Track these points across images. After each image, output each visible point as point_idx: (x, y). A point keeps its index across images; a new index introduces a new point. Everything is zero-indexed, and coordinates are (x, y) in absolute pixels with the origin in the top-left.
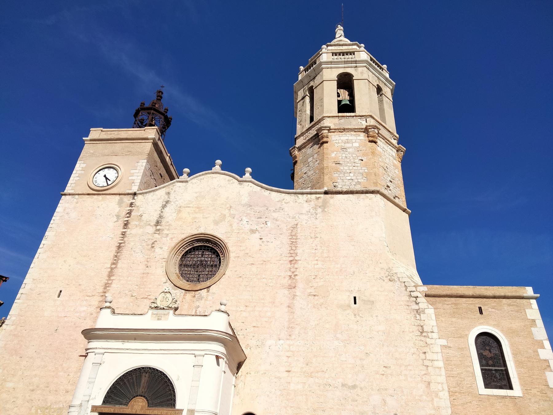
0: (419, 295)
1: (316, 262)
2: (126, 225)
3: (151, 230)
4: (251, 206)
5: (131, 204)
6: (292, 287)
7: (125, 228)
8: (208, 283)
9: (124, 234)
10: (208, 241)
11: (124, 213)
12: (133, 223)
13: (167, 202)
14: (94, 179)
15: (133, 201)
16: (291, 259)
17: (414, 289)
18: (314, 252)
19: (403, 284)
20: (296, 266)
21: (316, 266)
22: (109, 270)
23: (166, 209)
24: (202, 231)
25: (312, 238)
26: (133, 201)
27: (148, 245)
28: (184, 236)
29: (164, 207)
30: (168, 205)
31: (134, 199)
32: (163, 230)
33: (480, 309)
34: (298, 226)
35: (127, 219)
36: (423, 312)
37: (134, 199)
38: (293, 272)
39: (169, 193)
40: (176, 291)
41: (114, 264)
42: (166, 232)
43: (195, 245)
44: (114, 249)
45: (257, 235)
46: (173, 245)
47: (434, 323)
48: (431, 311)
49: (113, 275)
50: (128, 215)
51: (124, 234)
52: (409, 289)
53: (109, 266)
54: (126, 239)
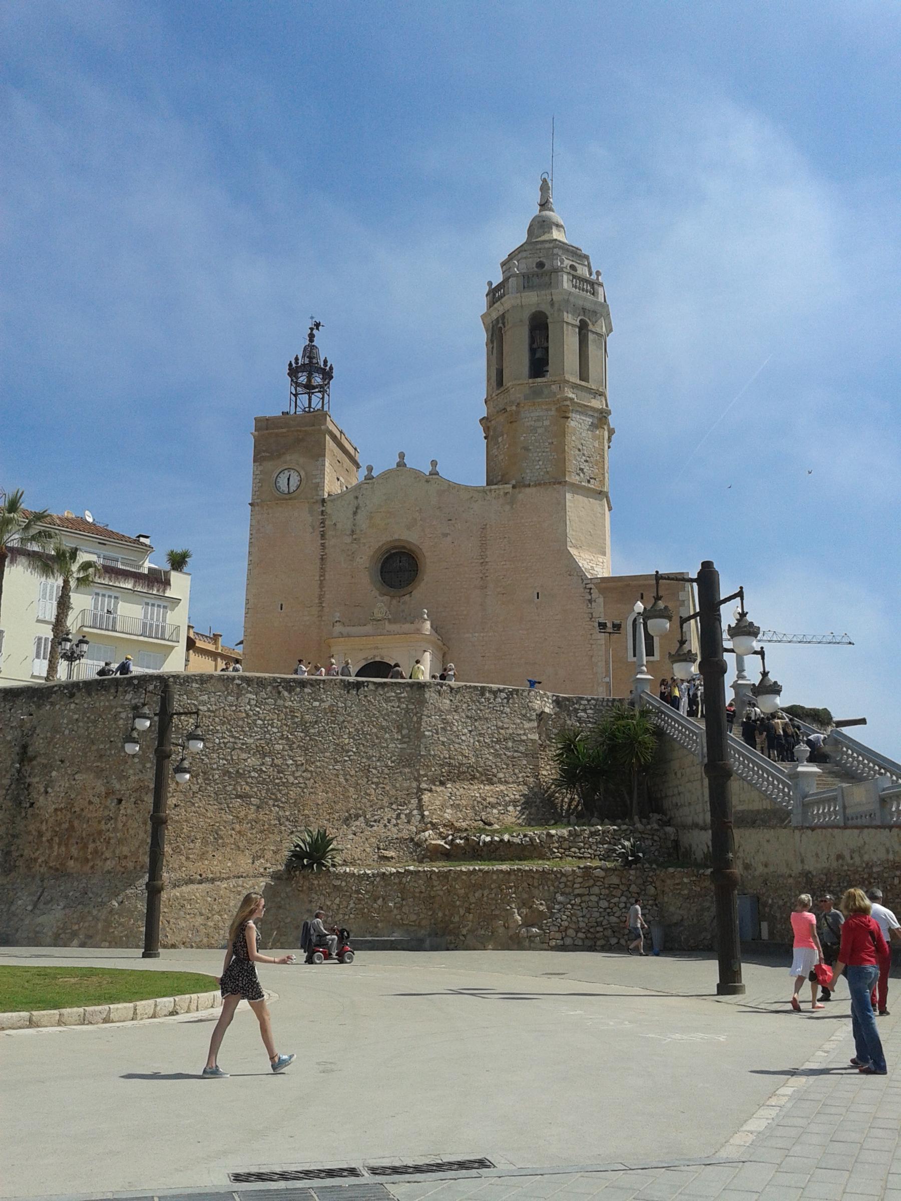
0: (592, 586)
1: (504, 563)
2: (323, 536)
3: (348, 540)
4: (440, 507)
5: (322, 511)
6: (484, 587)
7: (322, 539)
8: (409, 588)
9: (323, 545)
10: (404, 547)
11: (318, 523)
12: (330, 533)
13: (357, 508)
14: (278, 485)
15: (324, 508)
16: (482, 561)
17: (589, 582)
18: (502, 552)
19: (580, 578)
20: (487, 567)
21: (505, 567)
22: (319, 582)
23: (358, 517)
24: (396, 537)
25: (500, 538)
26: (324, 508)
27: (349, 556)
28: (380, 544)
29: (355, 513)
30: (359, 511)
31: (323, 506)
32: (359, 539)
33: (642, 594)
34: (488, 526)
35: (322, 529)
36: (595, 601)
37: (323, 506)
38: (484, 573)
39: (357, 498)
40: (382, 598)
41: (321, 576)
42: (362, 541)
43: (393, 552)
44: (318, 561)
45: (449, 539)
46: (372, 553)
47: (602, 609)
48: (601, 600)
49: (324, 587)
50: (322, 525)
51: (323, 545)
52: (585, 582)
53: (317, 578)
54: (326, 551)
